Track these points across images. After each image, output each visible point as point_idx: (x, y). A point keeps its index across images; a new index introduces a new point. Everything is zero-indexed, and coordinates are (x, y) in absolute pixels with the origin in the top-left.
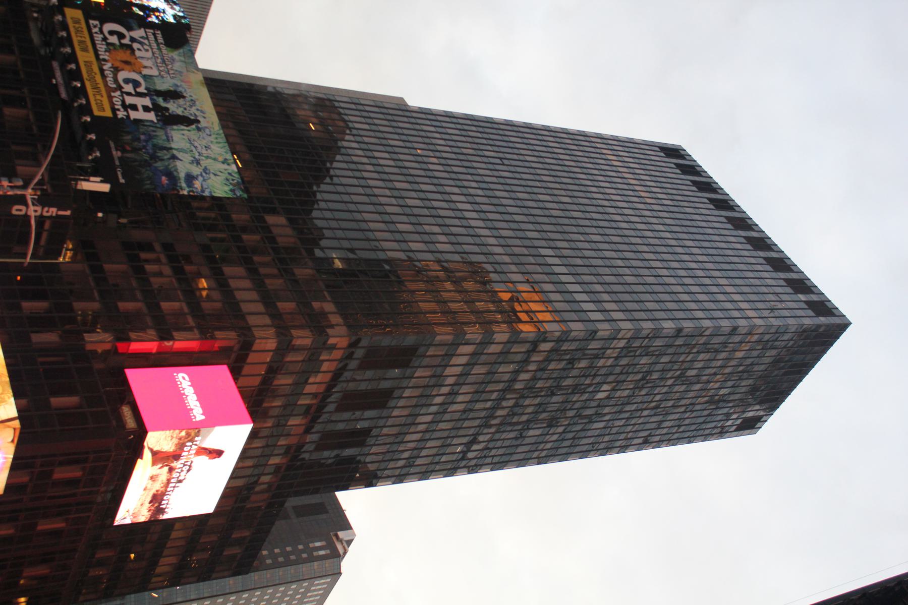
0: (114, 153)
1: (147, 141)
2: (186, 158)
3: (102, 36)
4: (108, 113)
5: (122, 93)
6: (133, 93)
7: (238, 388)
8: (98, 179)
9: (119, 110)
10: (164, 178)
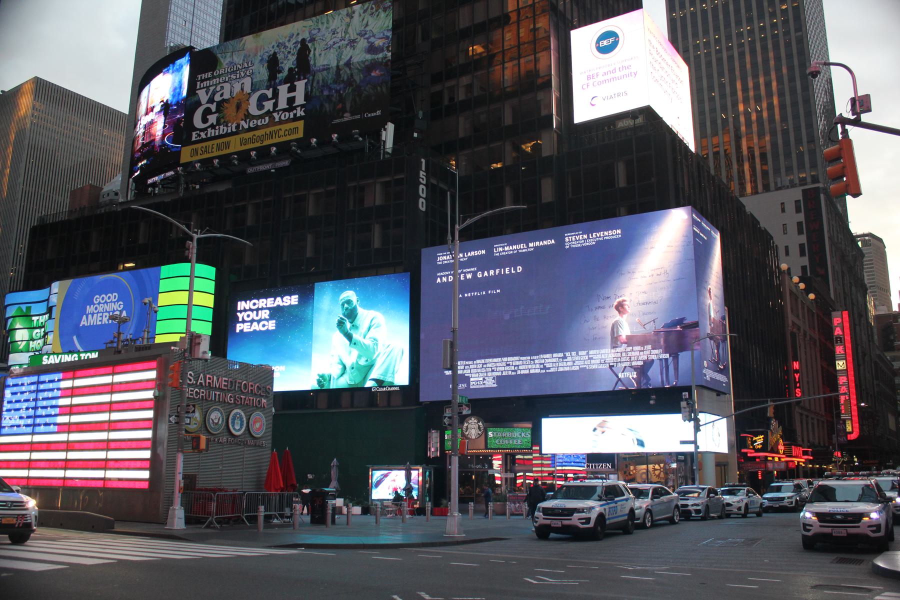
0: (346, 119)
1: (330, 89)
2: (347, 53)
3: (209, 130)
4: (300, 124)
5: (274, 111)
7: (580, 27)
8: (384, 133)
9: (295, 115)
10: (373, 74)
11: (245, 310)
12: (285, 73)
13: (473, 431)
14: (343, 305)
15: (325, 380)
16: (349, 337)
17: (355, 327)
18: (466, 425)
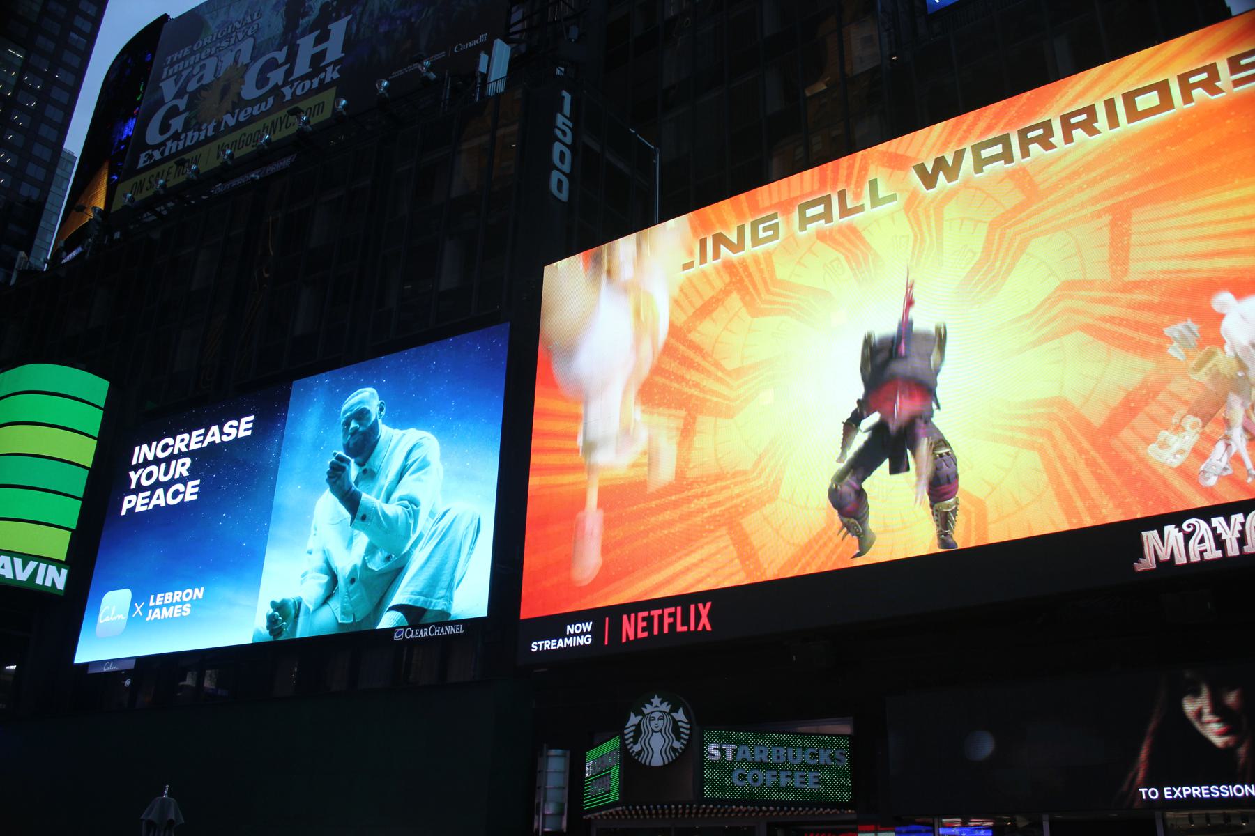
3: (169, 144)
5: (284, 85)
6: (288, 66)
8: (484, 58)
9: (322, 81)
11: (146, 463)
12: (315, 13)
13: (657, 742)
14: (347, 424)
16: (351, 501)
17: (369, 474)
18: (634, 720)
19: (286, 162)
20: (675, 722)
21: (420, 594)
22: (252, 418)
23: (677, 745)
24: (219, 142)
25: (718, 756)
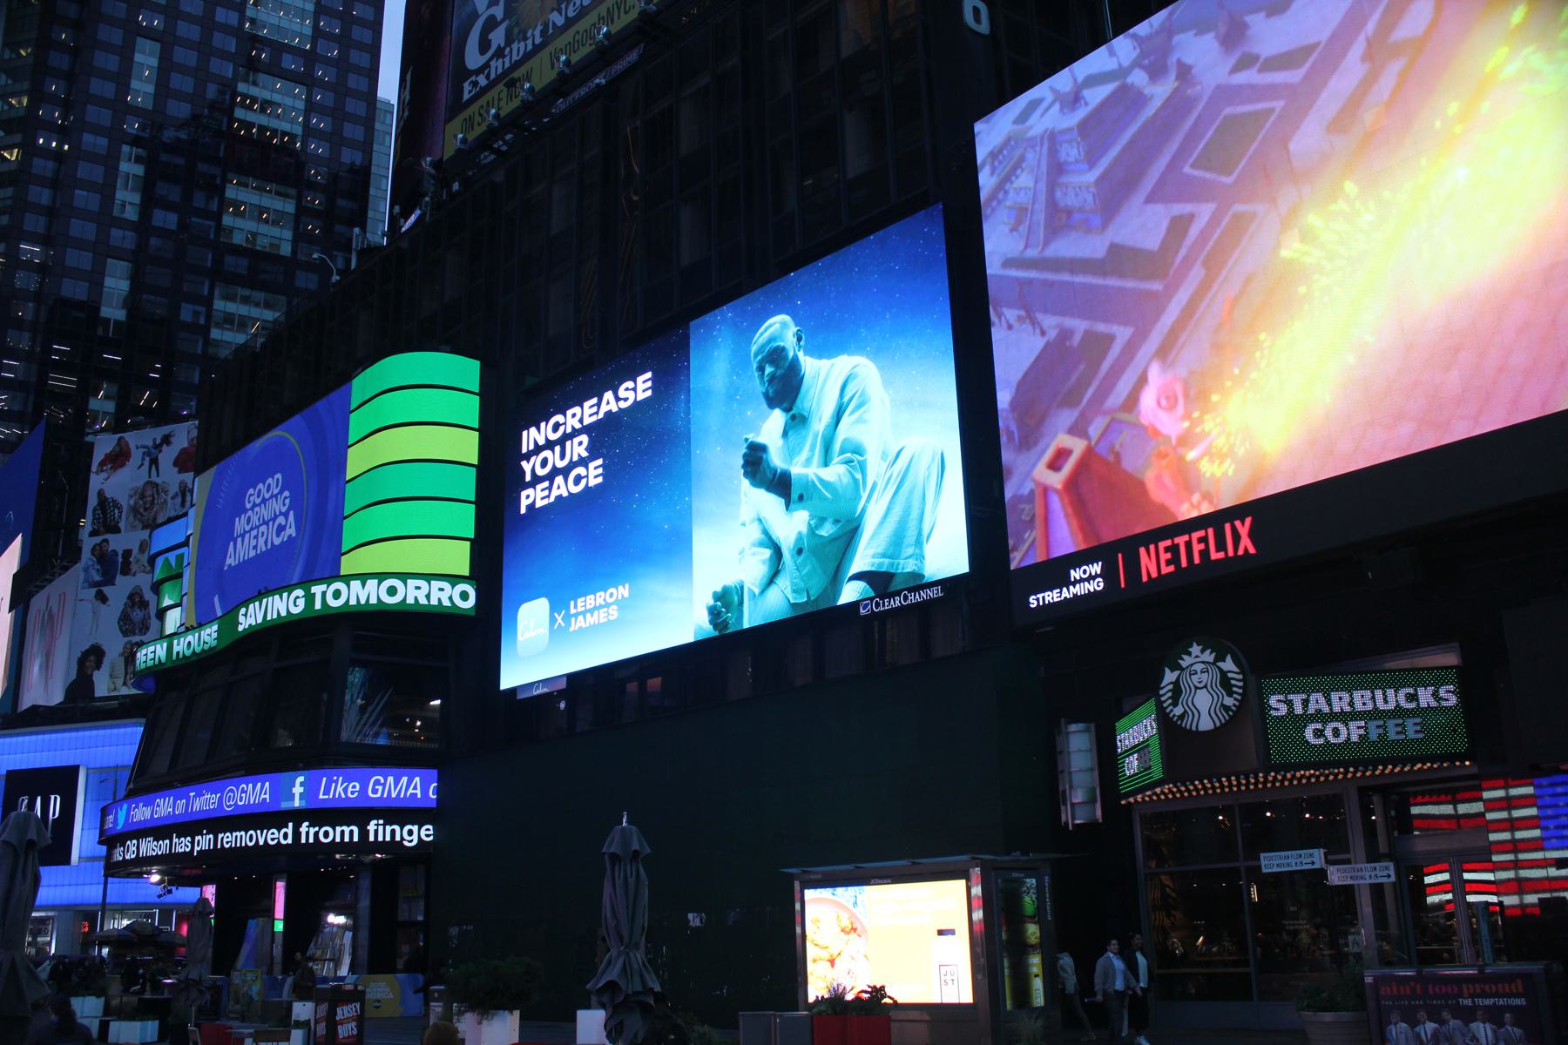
3: (493, 63)
11: (538, 449)
13: (1203, 701)
15: (727, 606)
18: (1170, 676)
19: (633, 56)
20: (1223, 674)
21: (884, 556)
22: (649, 375)
23: (1229, 701)
24: (550, 48)
25: (1283, 710)
